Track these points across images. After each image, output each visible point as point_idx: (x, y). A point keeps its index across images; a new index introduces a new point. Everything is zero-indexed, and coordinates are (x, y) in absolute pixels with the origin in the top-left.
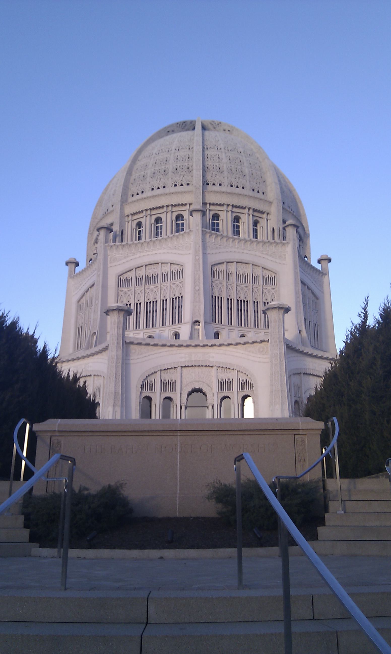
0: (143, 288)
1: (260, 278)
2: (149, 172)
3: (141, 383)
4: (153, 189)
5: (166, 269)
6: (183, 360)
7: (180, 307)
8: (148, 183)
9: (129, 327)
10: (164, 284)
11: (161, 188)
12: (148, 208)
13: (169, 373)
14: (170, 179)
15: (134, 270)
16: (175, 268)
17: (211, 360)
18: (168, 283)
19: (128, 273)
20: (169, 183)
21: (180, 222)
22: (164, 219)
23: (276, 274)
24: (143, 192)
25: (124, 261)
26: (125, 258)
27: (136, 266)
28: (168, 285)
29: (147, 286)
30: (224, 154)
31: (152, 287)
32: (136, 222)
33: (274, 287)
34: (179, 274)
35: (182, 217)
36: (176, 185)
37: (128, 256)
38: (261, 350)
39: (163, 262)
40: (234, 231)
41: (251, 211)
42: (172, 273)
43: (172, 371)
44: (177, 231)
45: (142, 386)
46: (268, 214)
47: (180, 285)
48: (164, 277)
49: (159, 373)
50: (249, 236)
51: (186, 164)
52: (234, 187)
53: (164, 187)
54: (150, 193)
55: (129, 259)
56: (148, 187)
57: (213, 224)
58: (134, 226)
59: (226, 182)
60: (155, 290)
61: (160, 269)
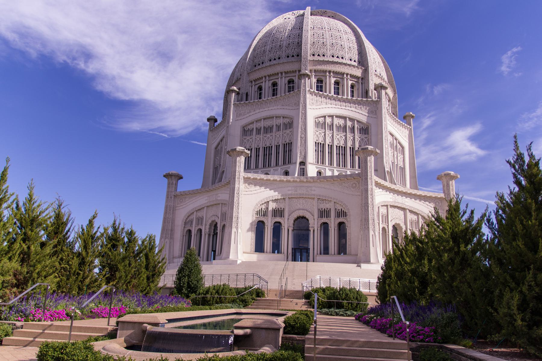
0: (262, 137)
2: (268, 48)
4: (270, 60)
5: (281, 121)
6: (290, 192)
7: (290, 151)
10: (278, 133)
11: (277, 59)
12: (266, 75)
14: (284, 52)
16: (286, 121)
17: (313, 192)
18: (281, 133)
19: (251, 125)
20: (284, 55)
22: (279, 83)
24: (263, 63)
25: (247, 115)
28: (281, 133)
29: (265, 135)
30: (327, 32)
31: (268, 135)
32: (257, 86)
33: (366, 136)
35: (293, 81)
36: (288, 57)
38: (354, 185)
39: (277, 115)
40: (335, 92)
41: (349, 76)
45: (258, 213)
48: (278, 127)
50: (347, 96)
51: (297, 40)
52: (335, 58)
53: (279, 58)
54: (268, 64)
55: (251, 114)
57: (317, 86)
58: (256, 89)
59: (329, 53)
60: (271, 137)
61: (274, 121)
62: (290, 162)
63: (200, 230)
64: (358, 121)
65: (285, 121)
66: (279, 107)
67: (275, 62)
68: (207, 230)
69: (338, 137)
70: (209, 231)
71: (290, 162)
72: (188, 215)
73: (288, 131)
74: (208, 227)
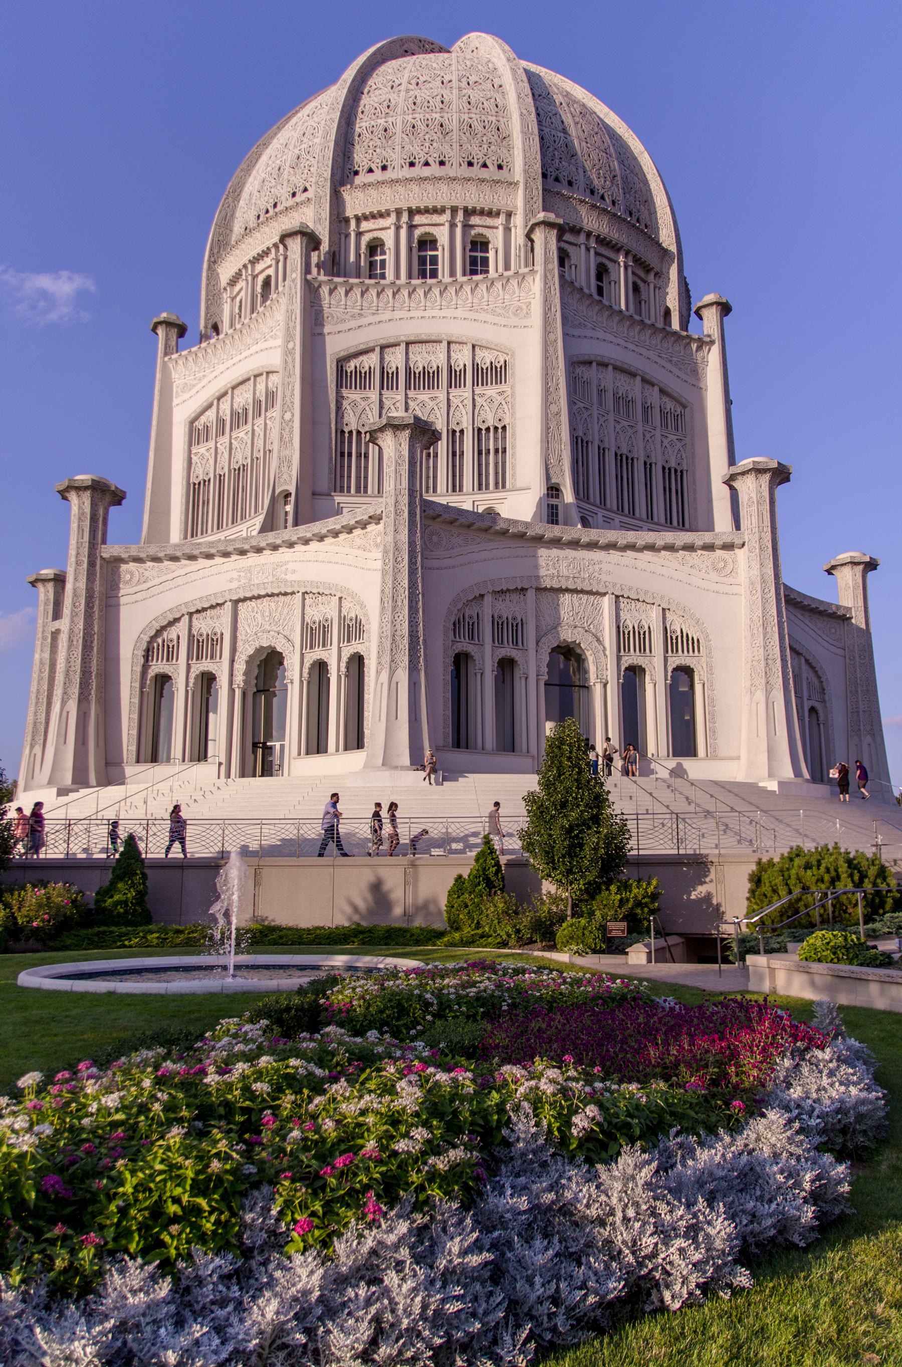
1: (656, 411)
2: (398, 121)
3: (453, 618)
5: (462, 358)
8: (398, 148)
9: (366, 487)
10: (454, 392)
13: (508, 601)
15: (378, 349)
16: (485, 358)
17: (604, 578)
20: (453, 154)
21: (479, 254)
23: (685, 407)
24: (384, 168)
25: (353, 324)
26: (353, 316)
27: (383, 342)
34: (497, 373)
37: (361, 315)
38: (722, 564)
39: (454, 339)
41: (630, 258)
42: (476, 367)
43: (515, 597)
44: (474, 272)
46: (656, 274)
47: (499, 398)
48: (455, 378)
49: (488, 599)
56: (396, 158)
62: (501, 484)
63: (208, 679)
64: (662, 391)
65: (478, 360)
66: (459, 313)
67: (426, 172)
68: (239, 679)
69: (618, 427)
70: (245, 681)
71: (501, 484)
72: (157, 626)
73: (491, 391)
74: (240, 667)
